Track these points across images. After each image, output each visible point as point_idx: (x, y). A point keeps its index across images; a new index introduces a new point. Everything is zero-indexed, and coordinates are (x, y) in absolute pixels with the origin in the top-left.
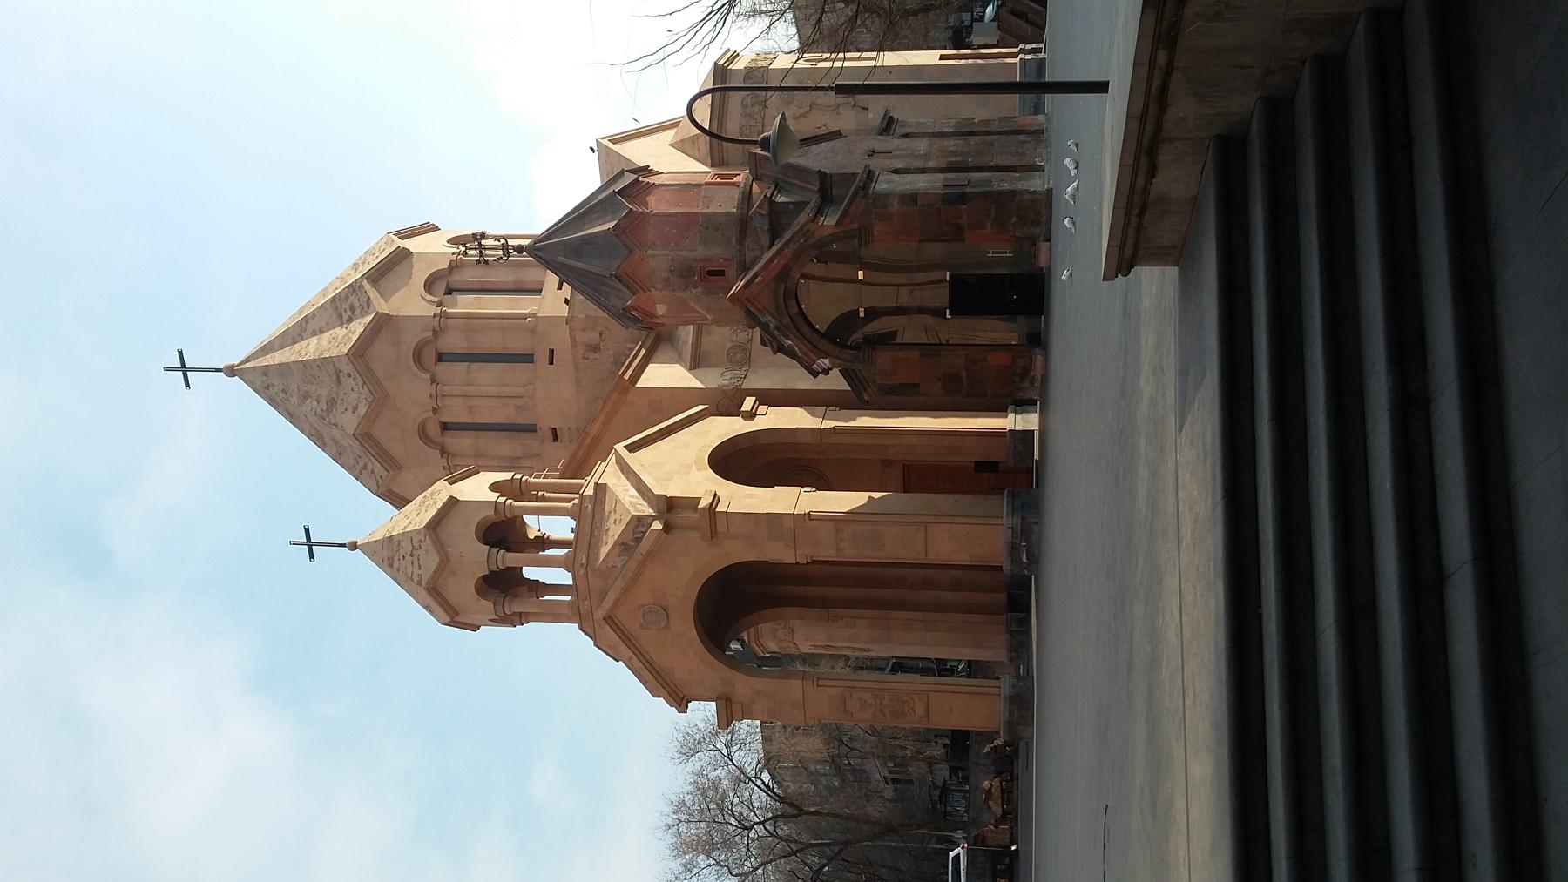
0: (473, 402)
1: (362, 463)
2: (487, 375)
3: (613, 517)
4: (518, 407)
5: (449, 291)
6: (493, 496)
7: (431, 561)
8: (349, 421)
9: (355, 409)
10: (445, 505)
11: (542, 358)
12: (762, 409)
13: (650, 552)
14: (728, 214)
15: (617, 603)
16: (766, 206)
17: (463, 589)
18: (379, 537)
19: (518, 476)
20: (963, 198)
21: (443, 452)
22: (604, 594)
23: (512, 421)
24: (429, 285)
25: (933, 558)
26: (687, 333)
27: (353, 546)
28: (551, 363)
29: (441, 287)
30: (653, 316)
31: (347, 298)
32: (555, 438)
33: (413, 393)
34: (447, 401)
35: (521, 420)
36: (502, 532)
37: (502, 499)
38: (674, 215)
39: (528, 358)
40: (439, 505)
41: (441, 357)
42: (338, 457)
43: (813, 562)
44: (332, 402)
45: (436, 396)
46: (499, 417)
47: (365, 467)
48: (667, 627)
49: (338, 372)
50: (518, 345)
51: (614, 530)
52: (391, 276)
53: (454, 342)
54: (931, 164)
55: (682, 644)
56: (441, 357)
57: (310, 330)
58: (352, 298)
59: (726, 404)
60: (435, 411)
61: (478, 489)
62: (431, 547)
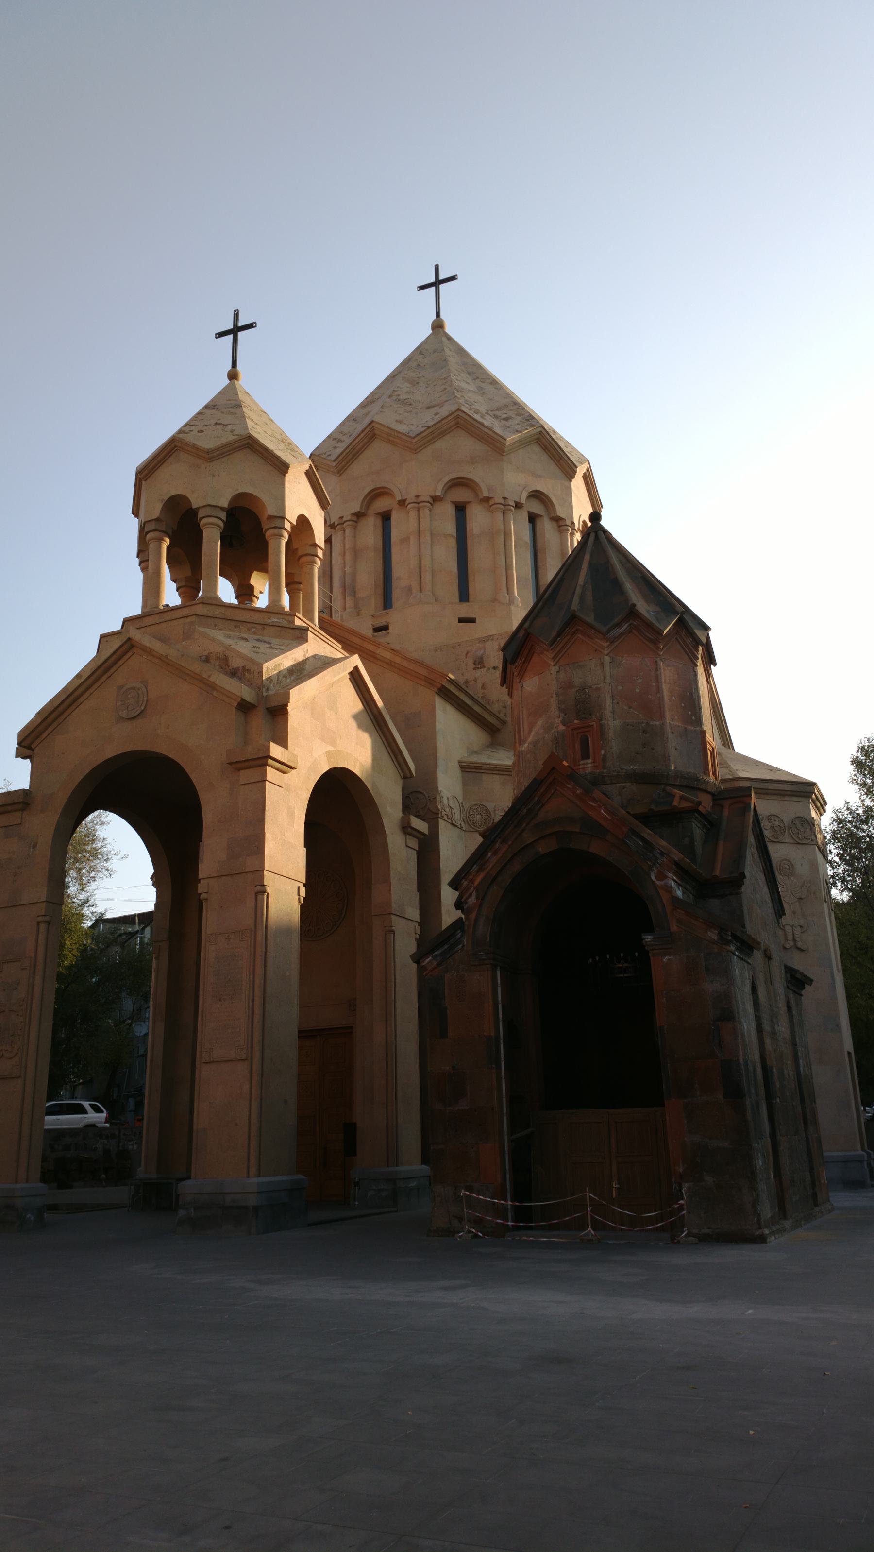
0: (413, 541)
1: (343, 438)
2: (445, 556)
3: (263, 647)
4: (409, 589)
5: (533, 519)
6: (292, 515)
7: (207, 443)
8: (389, 418)
9: (400, 422)
10: (278, 458)
11: (464, 610)
12: (414, 843)
13: (213, 687)
14: (666, 758)
15: (149, 652)
16: (685, 805)
17: (173, 482)
18: (241, 397)
19: (320, 553)
20: (735, 1093)
21: (359, 516)
22: (163, 640)
23: (395, 584)
24: (537, 495)
25: (204, 1072)
26: (504, 758)
27: (233, 376)
28: (461, 620)
29: (536, 508)
30: (522, 675)
31: (519, 415)
32: (377, 630)
33: (418, 478)
34: (413, 514)
35: (396, 593)
36: (248, 534)
37: (288, 526)
38: (659, 689)
39: (464, 596)
40: (278, 453)
41: (461, 509)
42: (352, 418)
43: (201, 903)
44: (405, 403)
45: (418, 502)
46: (399, 571)
47: (339, 441)
48: (120, 719)
49: (441, 405)
50: (479, 585)
51: (242, 648)
52: (545, 457)
53: (478, 519)
54: (768, 1041)
55: (101, 739)
56: (461, 509)
57: (483, 385)
58: (520, 418)
59: (418, 798)
60: (402, 503)
61: (299, 500)
62: (224, 440)
